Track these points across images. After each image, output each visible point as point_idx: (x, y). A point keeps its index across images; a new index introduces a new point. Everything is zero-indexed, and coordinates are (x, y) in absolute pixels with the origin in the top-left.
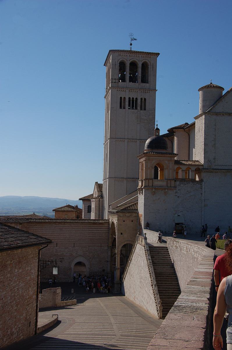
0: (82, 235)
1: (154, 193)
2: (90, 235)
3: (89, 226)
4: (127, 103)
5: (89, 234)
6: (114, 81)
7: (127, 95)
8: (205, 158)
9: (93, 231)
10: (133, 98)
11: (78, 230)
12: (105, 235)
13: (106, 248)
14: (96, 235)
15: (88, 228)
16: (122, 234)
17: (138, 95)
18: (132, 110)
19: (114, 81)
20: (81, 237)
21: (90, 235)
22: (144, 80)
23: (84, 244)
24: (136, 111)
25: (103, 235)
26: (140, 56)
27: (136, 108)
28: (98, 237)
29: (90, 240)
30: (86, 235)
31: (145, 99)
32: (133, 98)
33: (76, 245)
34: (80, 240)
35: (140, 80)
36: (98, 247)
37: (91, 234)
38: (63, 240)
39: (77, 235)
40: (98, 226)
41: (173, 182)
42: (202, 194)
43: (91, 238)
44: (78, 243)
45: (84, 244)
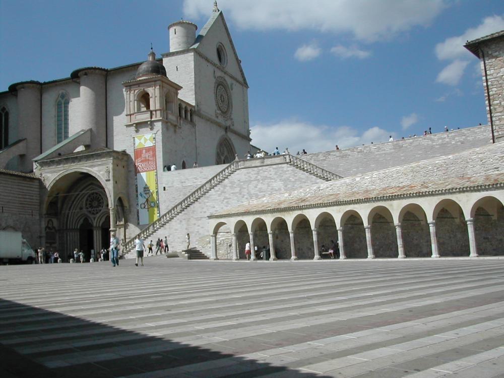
1: (167, 129)
3: (18, 183)
5: (19, 194)
8: (196, 99)
9: (24, 191)
11: (7, 187)
12: (36, 198)
13: (38, 217)
14: (27, 197)
15: (18, 185)
16: (116, 182)
20: (10, 198)
21: (20, 196)
25: (34, 198)
28: (29, 200)
29: (21, 204)
33: (5, 210)
34: (9, 202)
36: (29, 215)
39: (6, 194)
40: (29, 183)
42: (196, 139)
43: (21, 201)
44: (6, 207)
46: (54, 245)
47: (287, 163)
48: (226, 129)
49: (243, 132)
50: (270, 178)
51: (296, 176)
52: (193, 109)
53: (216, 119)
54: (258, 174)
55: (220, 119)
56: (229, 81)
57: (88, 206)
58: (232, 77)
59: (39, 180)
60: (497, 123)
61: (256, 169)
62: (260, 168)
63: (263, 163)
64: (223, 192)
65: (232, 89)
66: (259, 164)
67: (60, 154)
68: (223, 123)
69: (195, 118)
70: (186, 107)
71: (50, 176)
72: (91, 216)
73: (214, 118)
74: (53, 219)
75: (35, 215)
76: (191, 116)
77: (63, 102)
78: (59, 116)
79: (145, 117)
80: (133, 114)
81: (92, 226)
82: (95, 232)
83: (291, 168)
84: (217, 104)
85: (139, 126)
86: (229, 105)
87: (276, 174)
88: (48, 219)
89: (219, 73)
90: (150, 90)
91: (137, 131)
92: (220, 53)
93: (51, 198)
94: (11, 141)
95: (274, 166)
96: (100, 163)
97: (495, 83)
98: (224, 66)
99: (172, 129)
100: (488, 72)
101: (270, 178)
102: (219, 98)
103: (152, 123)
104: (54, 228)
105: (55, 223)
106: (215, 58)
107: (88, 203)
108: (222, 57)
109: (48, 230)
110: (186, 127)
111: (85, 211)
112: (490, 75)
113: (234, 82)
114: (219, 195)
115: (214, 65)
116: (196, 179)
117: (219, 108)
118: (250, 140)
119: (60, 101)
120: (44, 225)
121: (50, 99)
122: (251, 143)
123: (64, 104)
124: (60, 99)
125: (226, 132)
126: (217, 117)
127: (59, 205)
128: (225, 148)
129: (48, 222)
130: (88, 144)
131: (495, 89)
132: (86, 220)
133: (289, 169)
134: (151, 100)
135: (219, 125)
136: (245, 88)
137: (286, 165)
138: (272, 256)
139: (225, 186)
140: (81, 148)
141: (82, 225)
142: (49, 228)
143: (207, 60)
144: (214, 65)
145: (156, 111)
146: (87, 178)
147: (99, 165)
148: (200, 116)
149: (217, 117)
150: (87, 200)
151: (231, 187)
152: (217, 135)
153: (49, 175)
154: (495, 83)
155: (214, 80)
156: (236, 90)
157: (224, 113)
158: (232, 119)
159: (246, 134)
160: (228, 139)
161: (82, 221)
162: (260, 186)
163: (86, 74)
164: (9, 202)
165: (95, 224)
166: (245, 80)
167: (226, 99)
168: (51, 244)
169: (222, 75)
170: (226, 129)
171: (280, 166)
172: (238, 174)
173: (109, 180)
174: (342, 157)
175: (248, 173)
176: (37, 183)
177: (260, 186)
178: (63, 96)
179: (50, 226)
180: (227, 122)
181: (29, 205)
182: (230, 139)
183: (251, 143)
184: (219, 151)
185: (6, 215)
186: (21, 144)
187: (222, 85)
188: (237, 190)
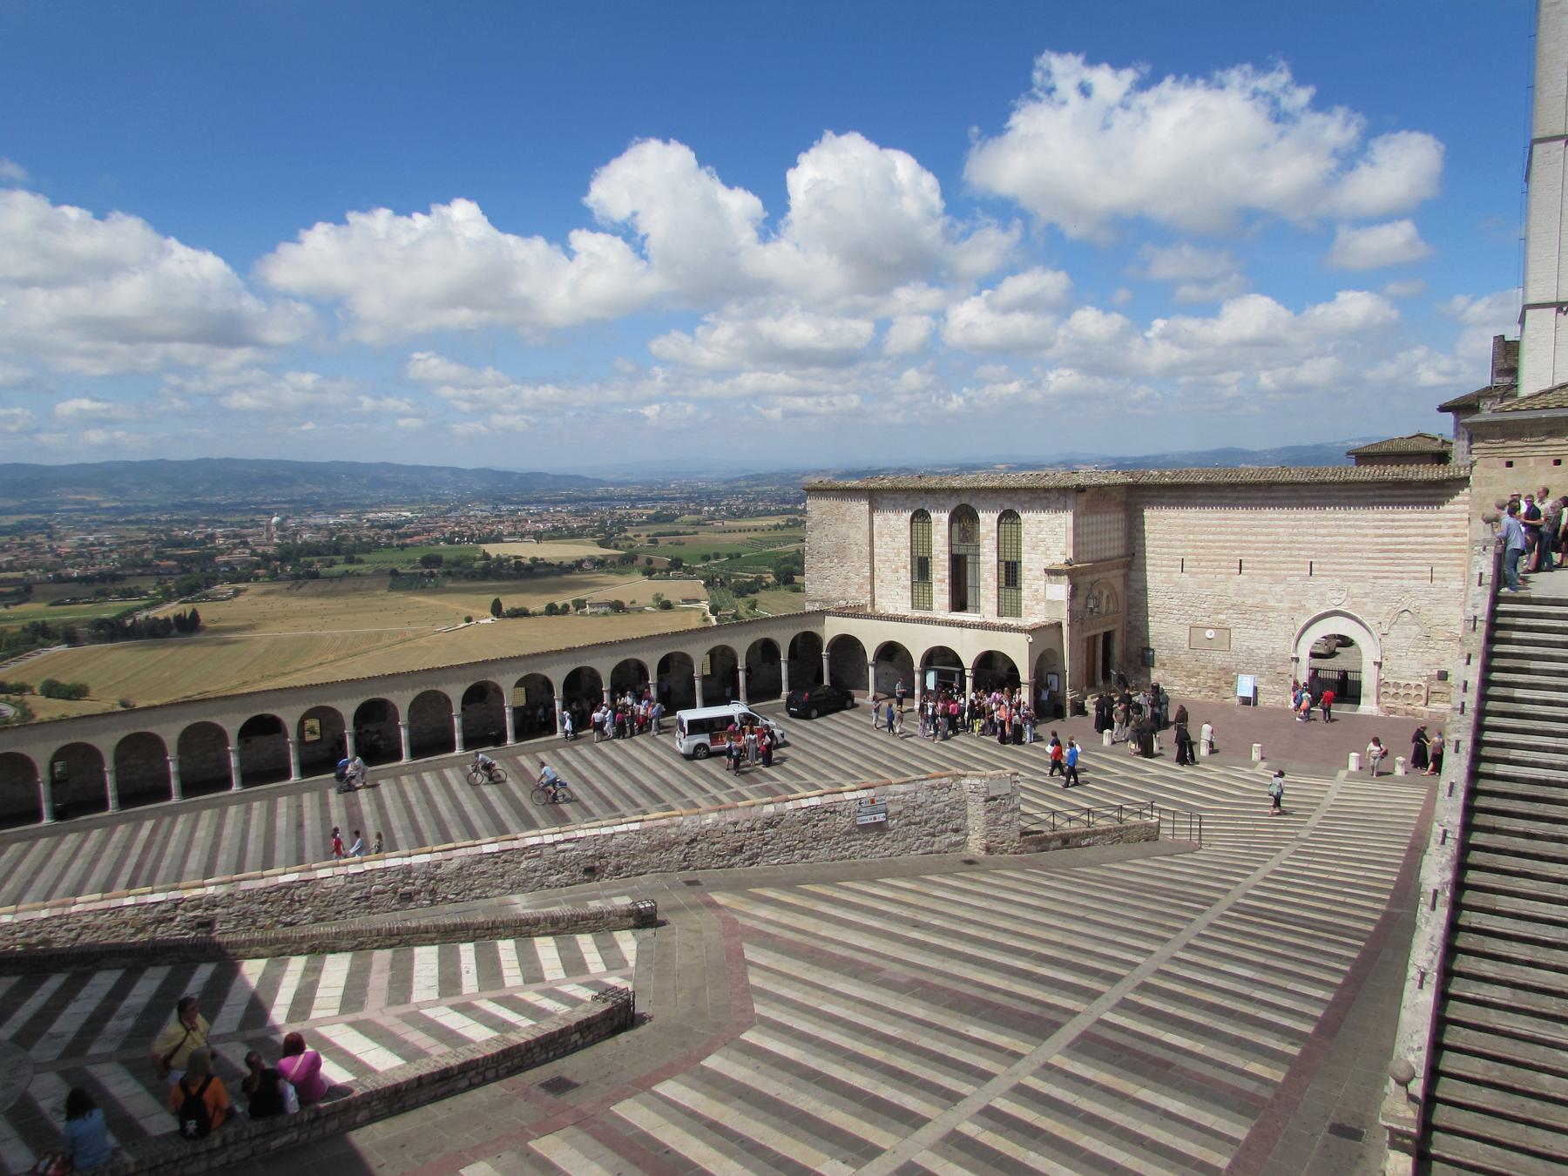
0: (1343, 530)
2: (1380, 532)
5: (1379, 527)
13: (1456, 584)
20: (1343, 539)
21: (1380, 532)
23: (1354, 567)
25: (1443, 531)
28: (1420, 539)
29: (1382, 551)
30: (1364, 531)
34: (1337, 550)
37: (1385, 527)
38: (1264, 549)
39: (1324, 531)
45: (1354, 567)
75: (1443, 579)
164: (1337, 550)
181: (1417, 551)
185: (1321, 581)
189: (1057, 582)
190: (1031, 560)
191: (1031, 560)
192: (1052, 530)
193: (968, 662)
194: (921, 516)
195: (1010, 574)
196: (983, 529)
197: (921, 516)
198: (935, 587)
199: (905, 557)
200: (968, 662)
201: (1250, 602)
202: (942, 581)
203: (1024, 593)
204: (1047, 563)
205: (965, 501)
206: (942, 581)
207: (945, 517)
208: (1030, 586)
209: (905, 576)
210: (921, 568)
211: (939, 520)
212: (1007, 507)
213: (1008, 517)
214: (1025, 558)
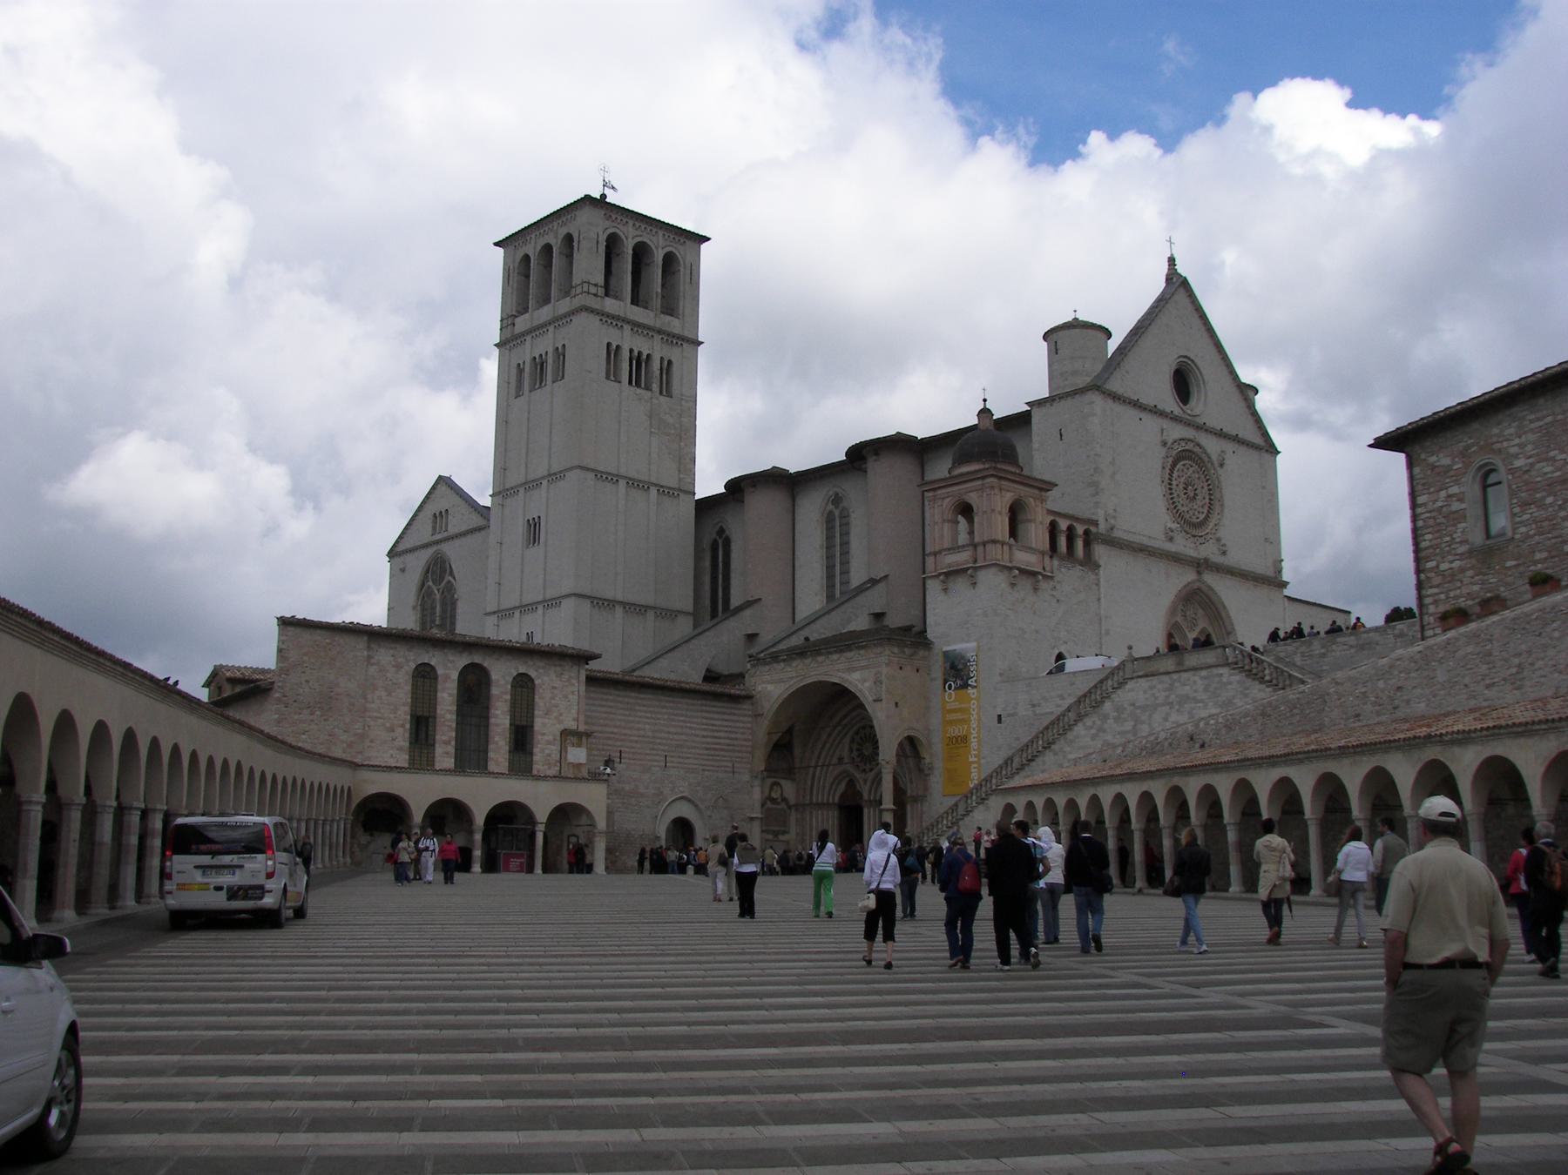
4: (625, 366)
6: (593, 290)
7: (629, 342)
10: (640, 353)
13: (746, 777)
17: (656, 349)
18: (639, 391)
19: (593, 290)
22: (670, 309)
24: (649, 394)
26: (661, 233)
27: (648, 388)
31: (670, 362)
32: (640, 353)
35: (657, 302)
41: (1047, 558)
46: (781, 837)
47: (1228, 665)
48: (1199, 565)
49: (1261, 567)
50: (1196, 701)
51: (1246, 696)
52: (1093, 529)
53: (1169, 547)
54: (1170, 689)
55: (1183, 545)
56: (1212, 446)
57: (855, 754)
58: (1221, 434)
59: (749, 697)
60: (1432, 609)
61: (1165, 678)
62: (1175, 676)
63: (1180, 663)
64: (1101, 730)
65: (1222, 465)
66: (1171, 668)
67: (807, 639)
68: (1193, 553)
69: (1100, 551)
70: (1070, 529)
71: (773, 687)
72: (858, 775)
73: (1161, 543)
74: (783, 782)
76: (1087, 544)
77: (837, 513)
78: (829, 547)
79: (963, 558)
80: (940, 552)
81: (861, 795)
82: (866, 811)
83: (1237, 678)
84: (1173, 506)
85: (951, 574)
86: (1213, 502)
87: (1206, 690)
88: (770, 781)
89: (1177, 432)
90: (973, 499)
91: (945, 590)
92: (1183, 382)
93: (775, 738)
94: (735, 601)
95: (1204, 673)
96: (863, 663)
97: (1431, 522)
98: (1197, 411)
99: (1026, 583)
100: (1420, 500)
101: (1196, 701)
102: (1178, 491)
103: (976, 569)
104: (784, 800)
105: (789, 789)
106: (1169, 402)
107: (855, 746)
108: (1193, 389)
109: (769, 804)
110: (1069, 578)
111: (850, 768)
112: (1424, 504)
113: (1229, 447)
114: (1094, 737)
115: (1162, 414)
116: (1062, 698)
117: (1179, 516)
118: (1284, 585)
119: (831, 512)
120: (757, 794)
121: (811, 507)
122: (1287, 592)
123: (841, 517)
124: (831, 507)
125: (1199, 573)
126: (1171, 539)
127: (797, 751)
128: (1201, 612)
129: (771, 789)
130: (878, 610)
131: (1428, 537)
132: (851, 783)
133: (1233, 678)
134: (976, 520)
135: (1176, 559)
136: (1267, 456)
137: (1224, 671)
138: (477, 868)
139: (1105, 717)
140: (861, 623)
141: (842, 796)
142: (773, 800)
143: (1136, 404)
144: (1162, 414)
145: (984, 544)
146: (839, 697)
147: (862, 668)
148: (1112, 542)
149: (1171, 539)
150: (853, 740)
151: (1117, 719)
152: (1171, 583)
153: (770, 687)
154: (1431, 522)
155: (1163, 451)
156: (1236, 466)
157: (1194, 527)
158: (1218, 540)
159: (1270, 573)
160: (1205, 589)
161: (843, 786)
162: (1174, 717)
163: (877, 454)
165: (866, 796)
166: (1265, 434)
167: (1203, 493)
168: (776, 834)
169: (1189, 433)
170: (1201, 565)
171: (1215, 671)
172: (1132, 690)
173: (878, 700)
174: (1362, 648)
175: (1151, 688)
176: (746, 706)
177: (1174, 717)
178: (837, 500)
179: (774, 795)
180: (1202, 548)
182: (1211, 589)
183: (1287, 592)
184: (1179, 619)
186: (747, 613)
187: (1190, 458)
188: (1128, 726)
189: (579, 745)
190: (544, 725)
191: (544, 725)
192: (566, 697)
193: (542, 816)
194: (425, 674)
195: (522, 739)
196: (495, 691)
197: (425, 674)
198: (439, 750)
199: (404, 715)
200: (542, 816)
201: (627, 788)
202: (447, 743)
203: (535, 758)
204: (562, 727)
205: (477, 659)
206: (447, 743)
207: (455, 675)
208: (542, 751)
209: (402, 737)
210: (422, 727)
211: (447, 677)
212: (522, 670)
213: (523, 684)
214: (538, 724)
